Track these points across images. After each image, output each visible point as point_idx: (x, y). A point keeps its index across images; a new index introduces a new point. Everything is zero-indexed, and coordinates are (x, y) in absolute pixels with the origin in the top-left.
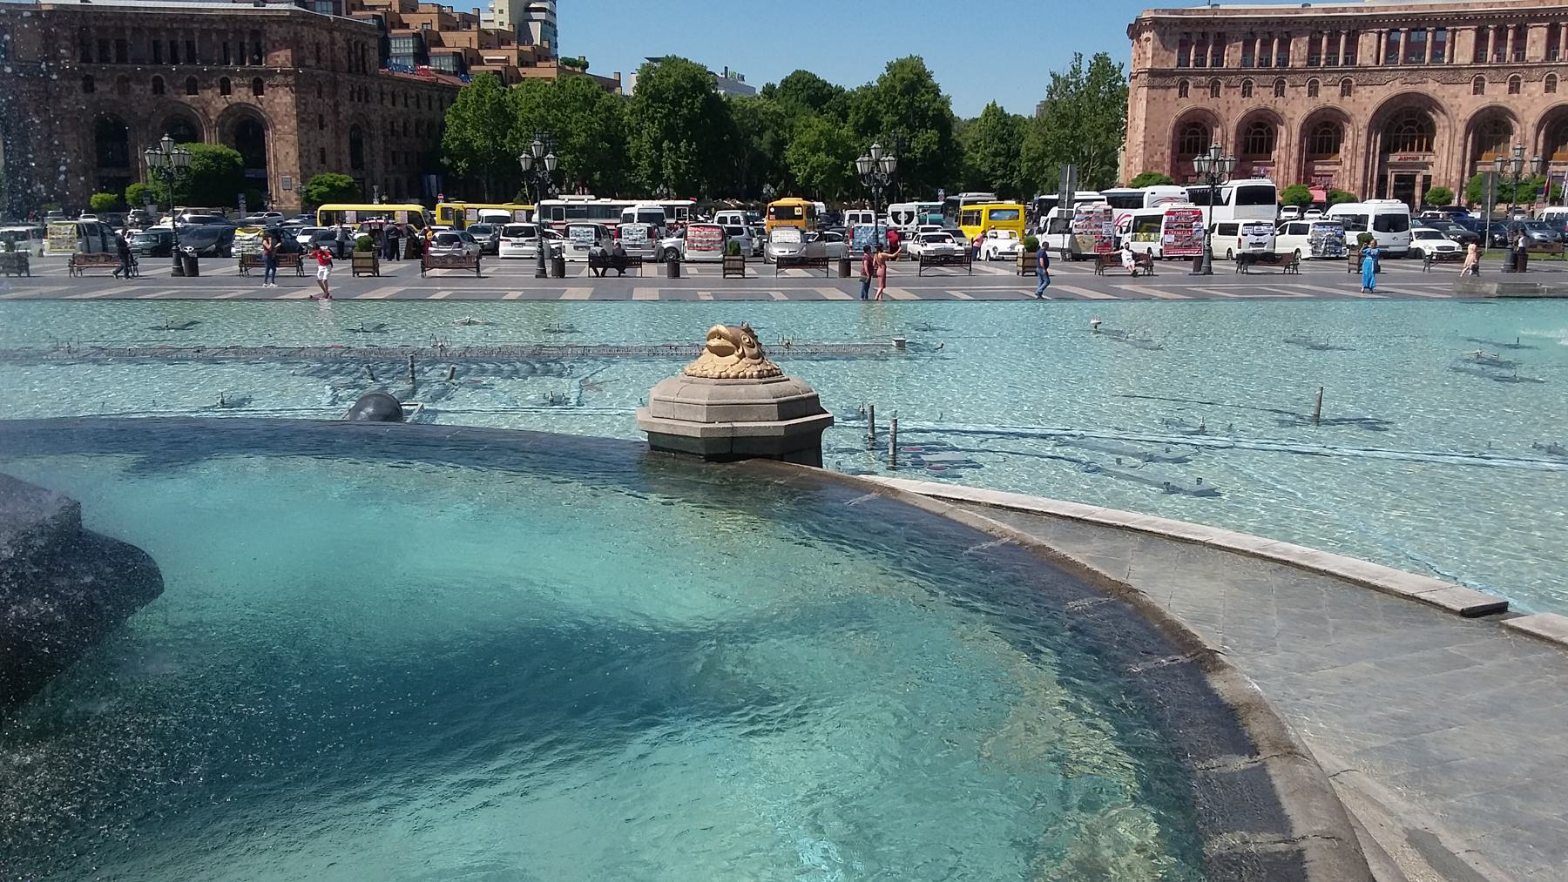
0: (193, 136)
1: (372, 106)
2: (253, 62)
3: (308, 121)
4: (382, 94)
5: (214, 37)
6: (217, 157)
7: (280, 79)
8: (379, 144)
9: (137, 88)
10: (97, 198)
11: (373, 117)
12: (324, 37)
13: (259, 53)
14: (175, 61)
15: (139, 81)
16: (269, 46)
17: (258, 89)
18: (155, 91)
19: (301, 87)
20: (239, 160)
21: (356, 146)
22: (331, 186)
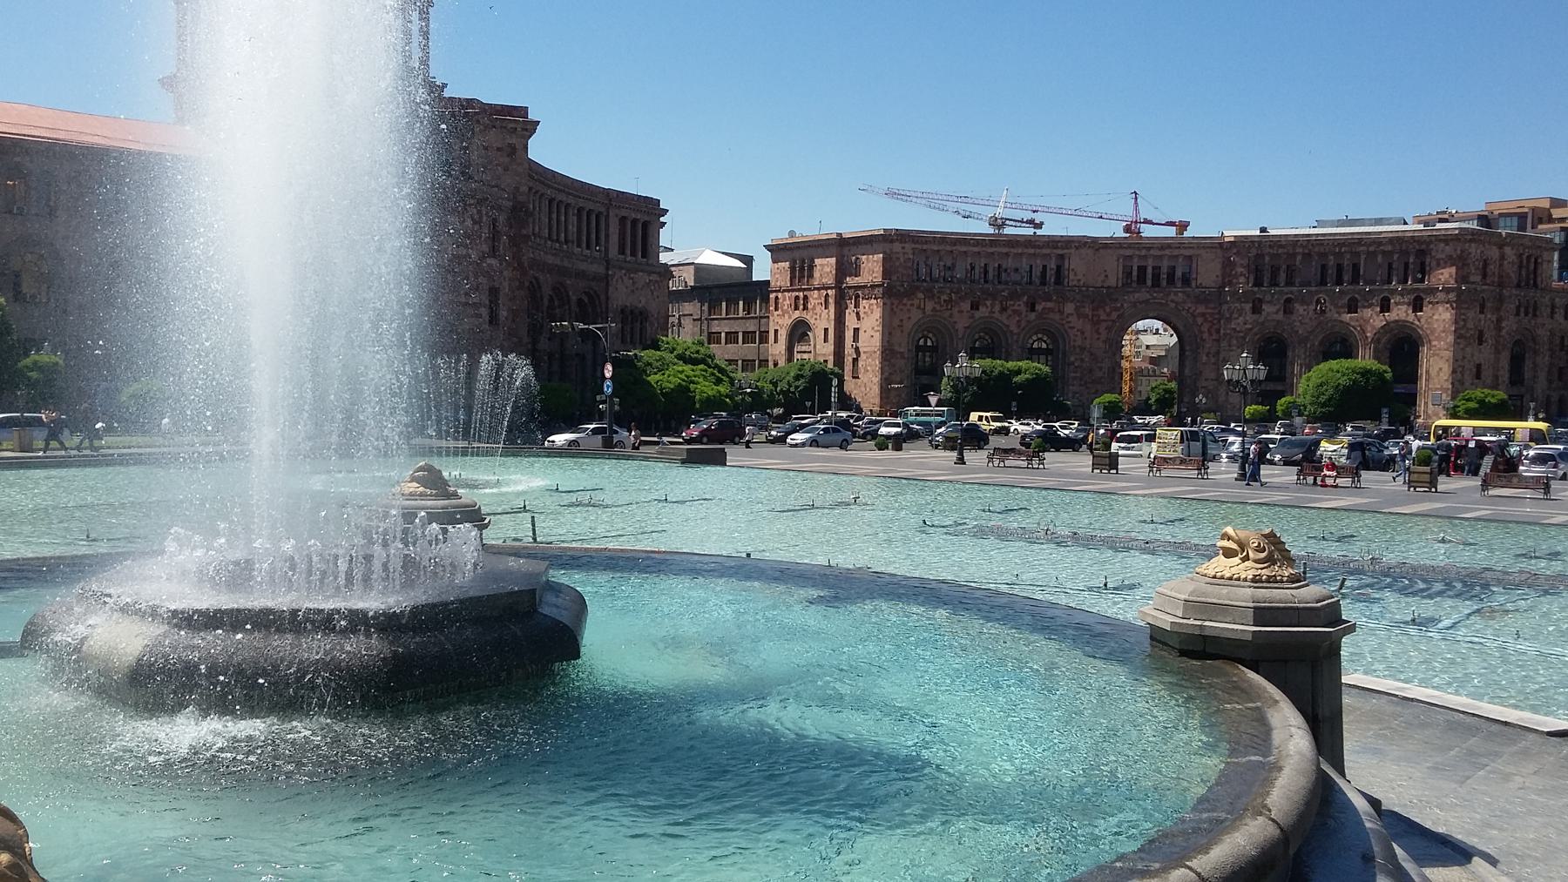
0: (1349, 353)
1: (1539, 320)
2: (1415, 281)
3: (1464, 336)
4: (1553, 307)
5: (1380, 258)
6: (1366, 373)
7: (1441, 296)
8: (1544, 360)
9: (1300, 309)
10: (1250, 409)
11: (1540, 332)
12: (1494, 253)
13: (1423, 271)
14: (1339, 282)
15: (1303, 303)
16: (1434, 263)
17: (1417, 306)
19: (1462, 301)
20: (1389, 376)
21: (1517, 362)
22: (1481, 402)
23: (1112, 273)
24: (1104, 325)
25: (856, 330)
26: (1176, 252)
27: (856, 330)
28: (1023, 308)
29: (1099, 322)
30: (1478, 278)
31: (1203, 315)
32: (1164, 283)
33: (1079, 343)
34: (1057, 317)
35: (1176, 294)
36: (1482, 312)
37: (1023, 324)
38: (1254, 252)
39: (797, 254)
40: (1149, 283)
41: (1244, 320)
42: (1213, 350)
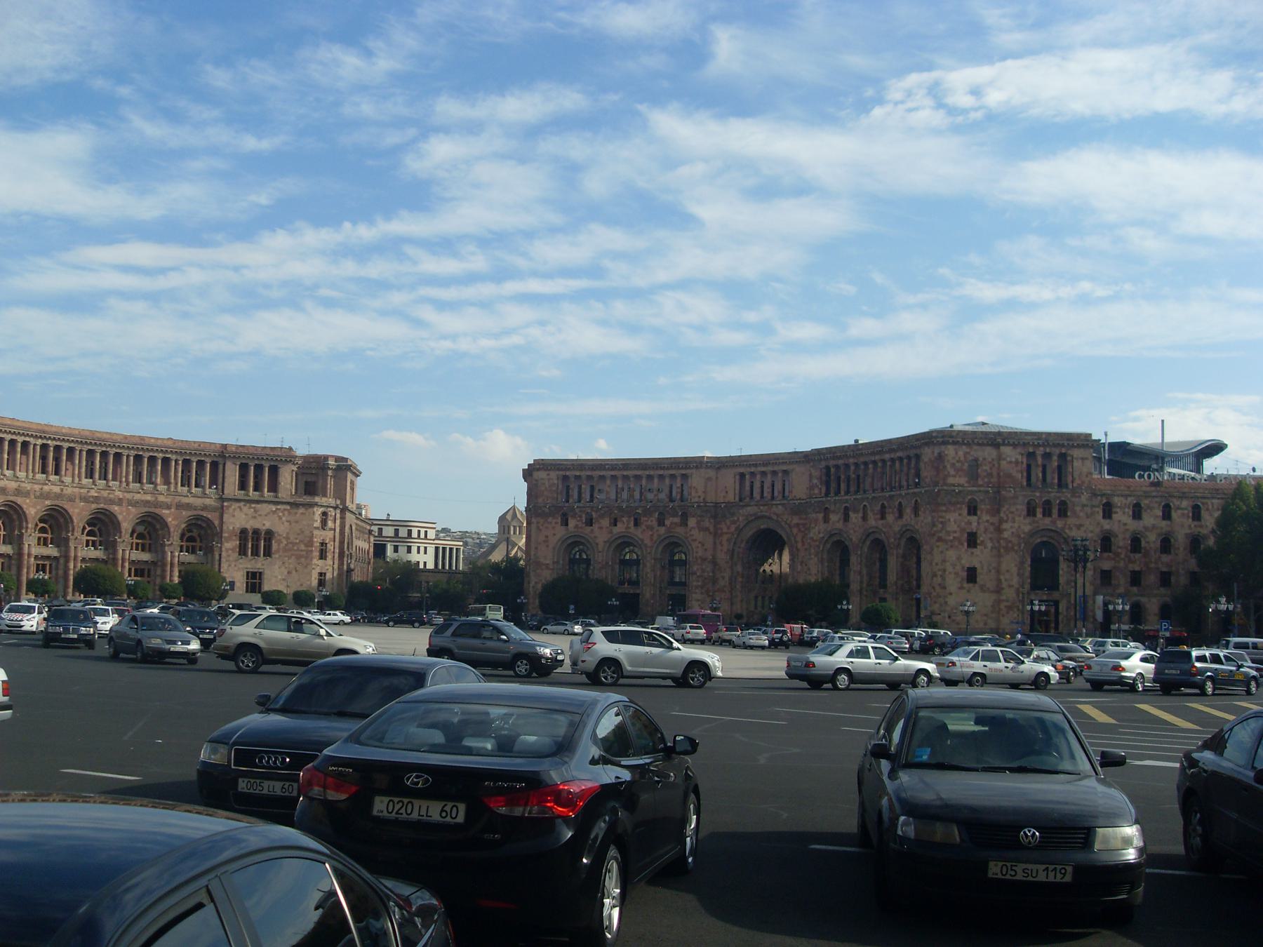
1: (1071, 521)
15: (856, 511)
17: (916, 510)
23: (728, 485)
24: (725, 537)
26: (776, 468)
28: (655, 523)
29: (722, 534)
30: (963, 481)
31: (798, 525)
33: (700, 554)
34: (680, 531)
36: (973, 510)
37: (655, 538)
38: (823, 464)
41: (818, 531)
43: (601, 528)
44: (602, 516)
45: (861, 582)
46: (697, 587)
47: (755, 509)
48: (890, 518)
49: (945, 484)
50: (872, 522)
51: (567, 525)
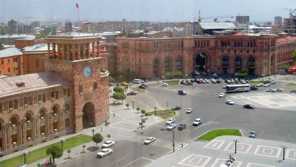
9: (231, 51)
17: (254, 51)
18: (234, 52)
25: (140, 60)
27: (140, 60)
28: (175, 52)
31: (212, 52)
32: (204, 46)
35: (206, 48)
36: (266, 52)
37: (175, 56)
38: (222, 40)
39: (123, 41)
40: (201, 46)
41: (220, 54)
42: (214, 60)
43: (163, 54)
44: (163, 51)
45: (234, 65)
46: (186, 67)
47: (200, 49)
48: (244, 52)
49: (263, 47)
50: (238, 53)
51: (155, 54)
